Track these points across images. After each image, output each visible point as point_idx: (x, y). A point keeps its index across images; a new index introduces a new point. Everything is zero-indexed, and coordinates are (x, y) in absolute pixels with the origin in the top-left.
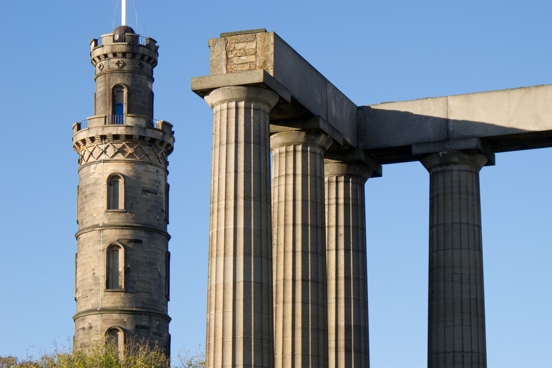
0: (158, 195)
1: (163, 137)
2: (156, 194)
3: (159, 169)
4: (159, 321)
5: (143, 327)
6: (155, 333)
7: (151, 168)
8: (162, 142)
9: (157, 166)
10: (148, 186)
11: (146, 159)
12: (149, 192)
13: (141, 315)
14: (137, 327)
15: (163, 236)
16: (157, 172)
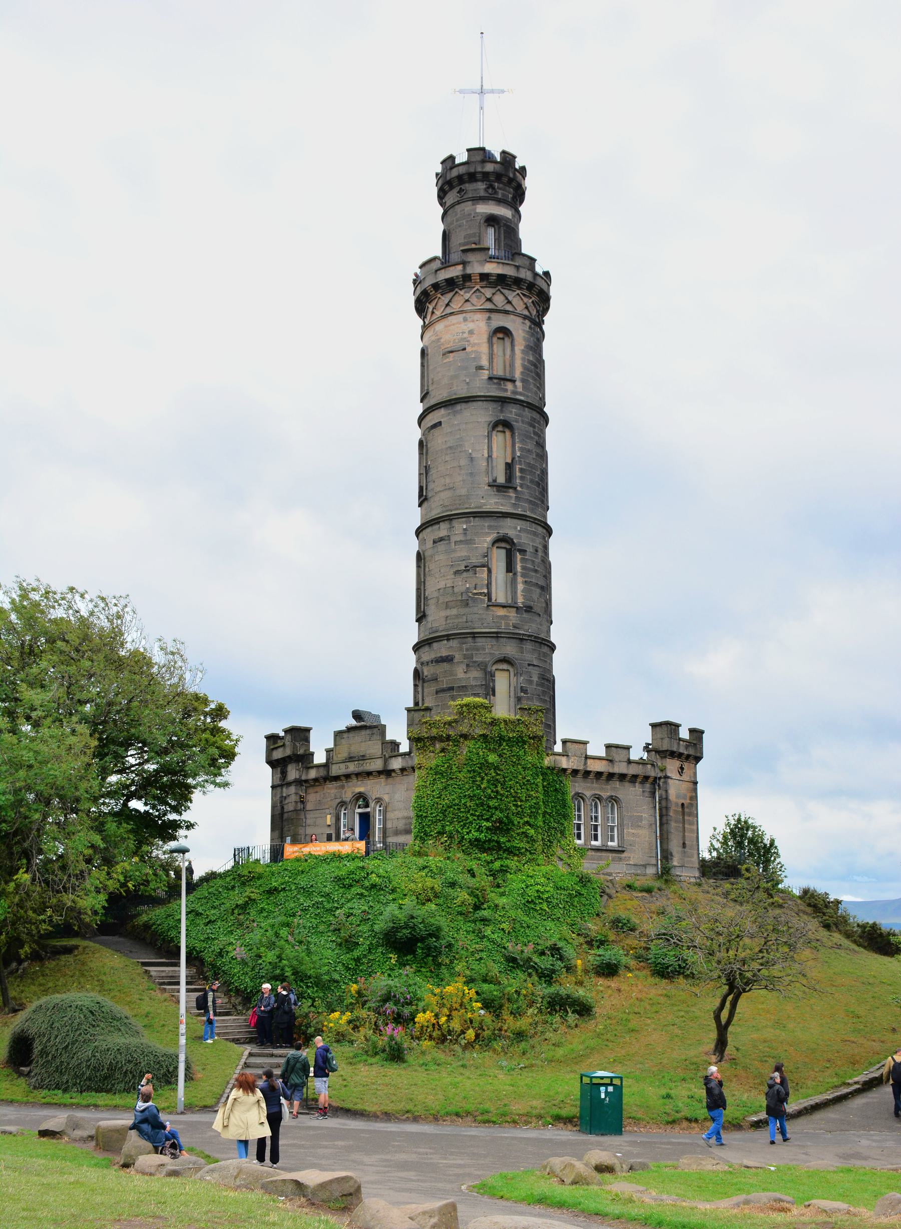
0: (468, 349)
1: (464, 268)
2: (464, 349)
3: (468, 315)
4: (466, 522)
5: (441, 539)
6: (461, 541)
7: (452, 319)
8: (467, 278)
9: (462, 312)
10: (450, 346)
11: (448, 310)
12: (452, 352)
13: (438, 523)
14: (434, 542)
15: (480, 403)
16: (465, 320)
